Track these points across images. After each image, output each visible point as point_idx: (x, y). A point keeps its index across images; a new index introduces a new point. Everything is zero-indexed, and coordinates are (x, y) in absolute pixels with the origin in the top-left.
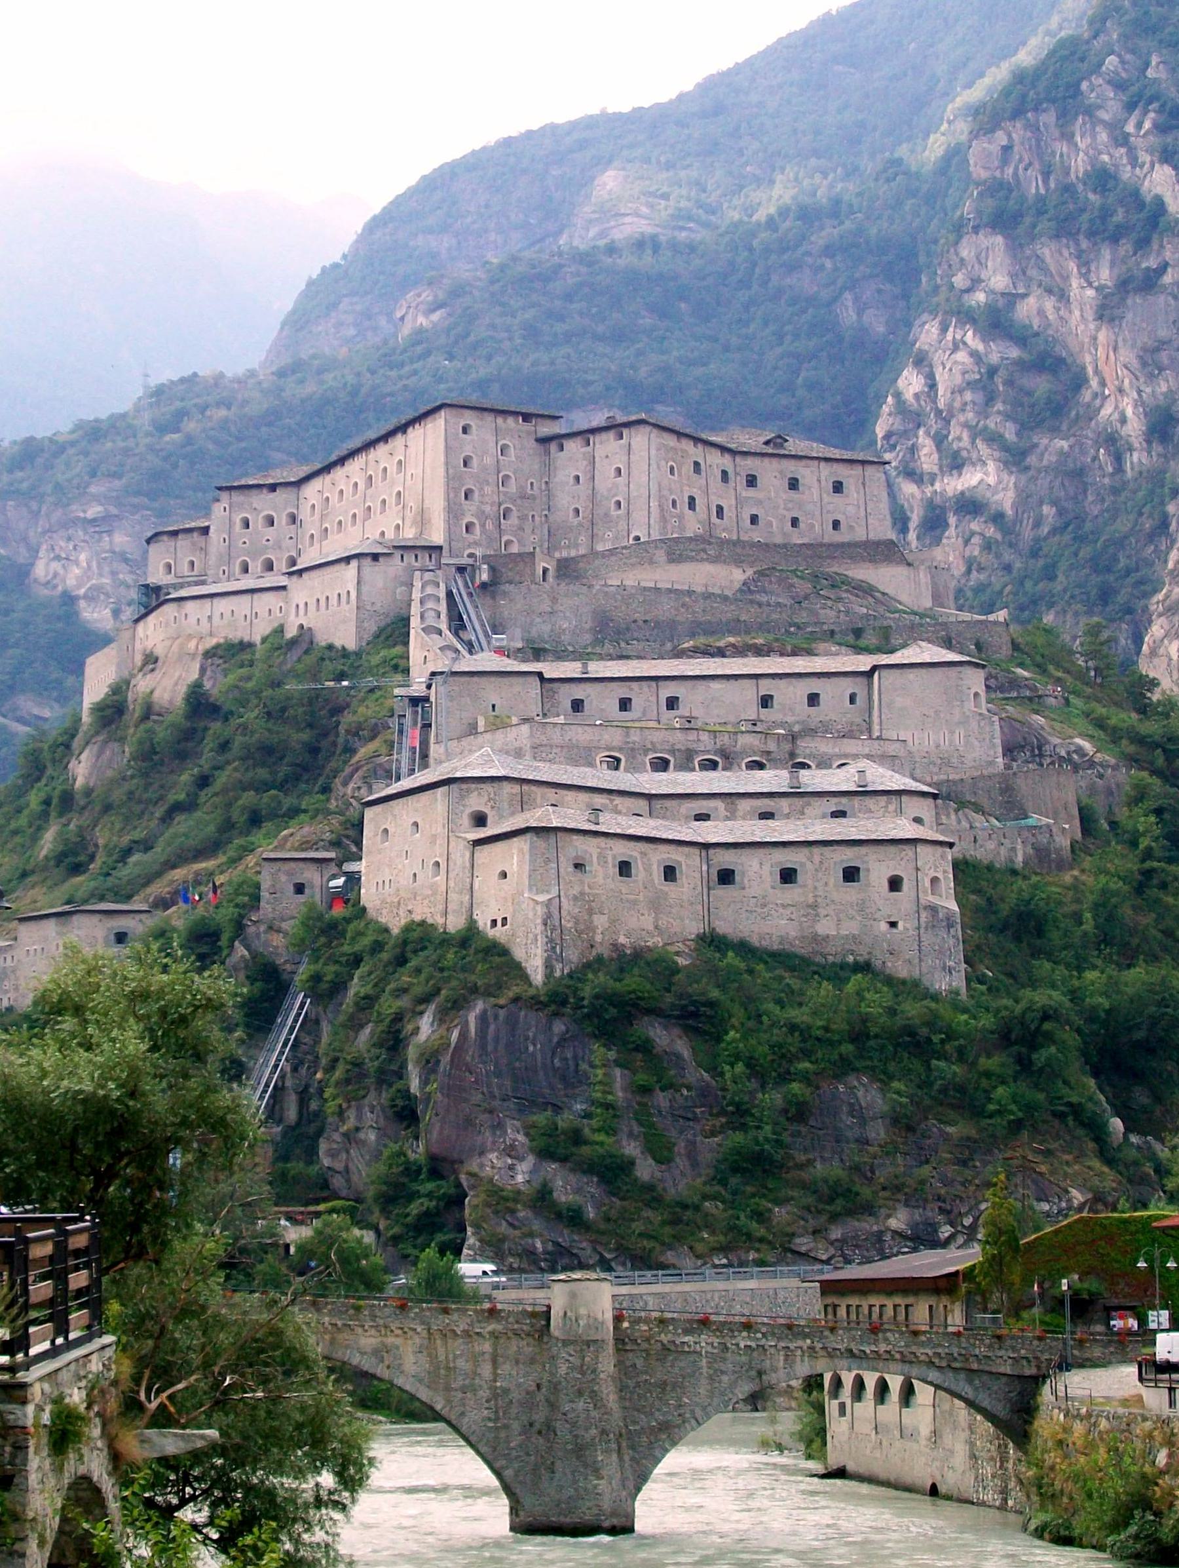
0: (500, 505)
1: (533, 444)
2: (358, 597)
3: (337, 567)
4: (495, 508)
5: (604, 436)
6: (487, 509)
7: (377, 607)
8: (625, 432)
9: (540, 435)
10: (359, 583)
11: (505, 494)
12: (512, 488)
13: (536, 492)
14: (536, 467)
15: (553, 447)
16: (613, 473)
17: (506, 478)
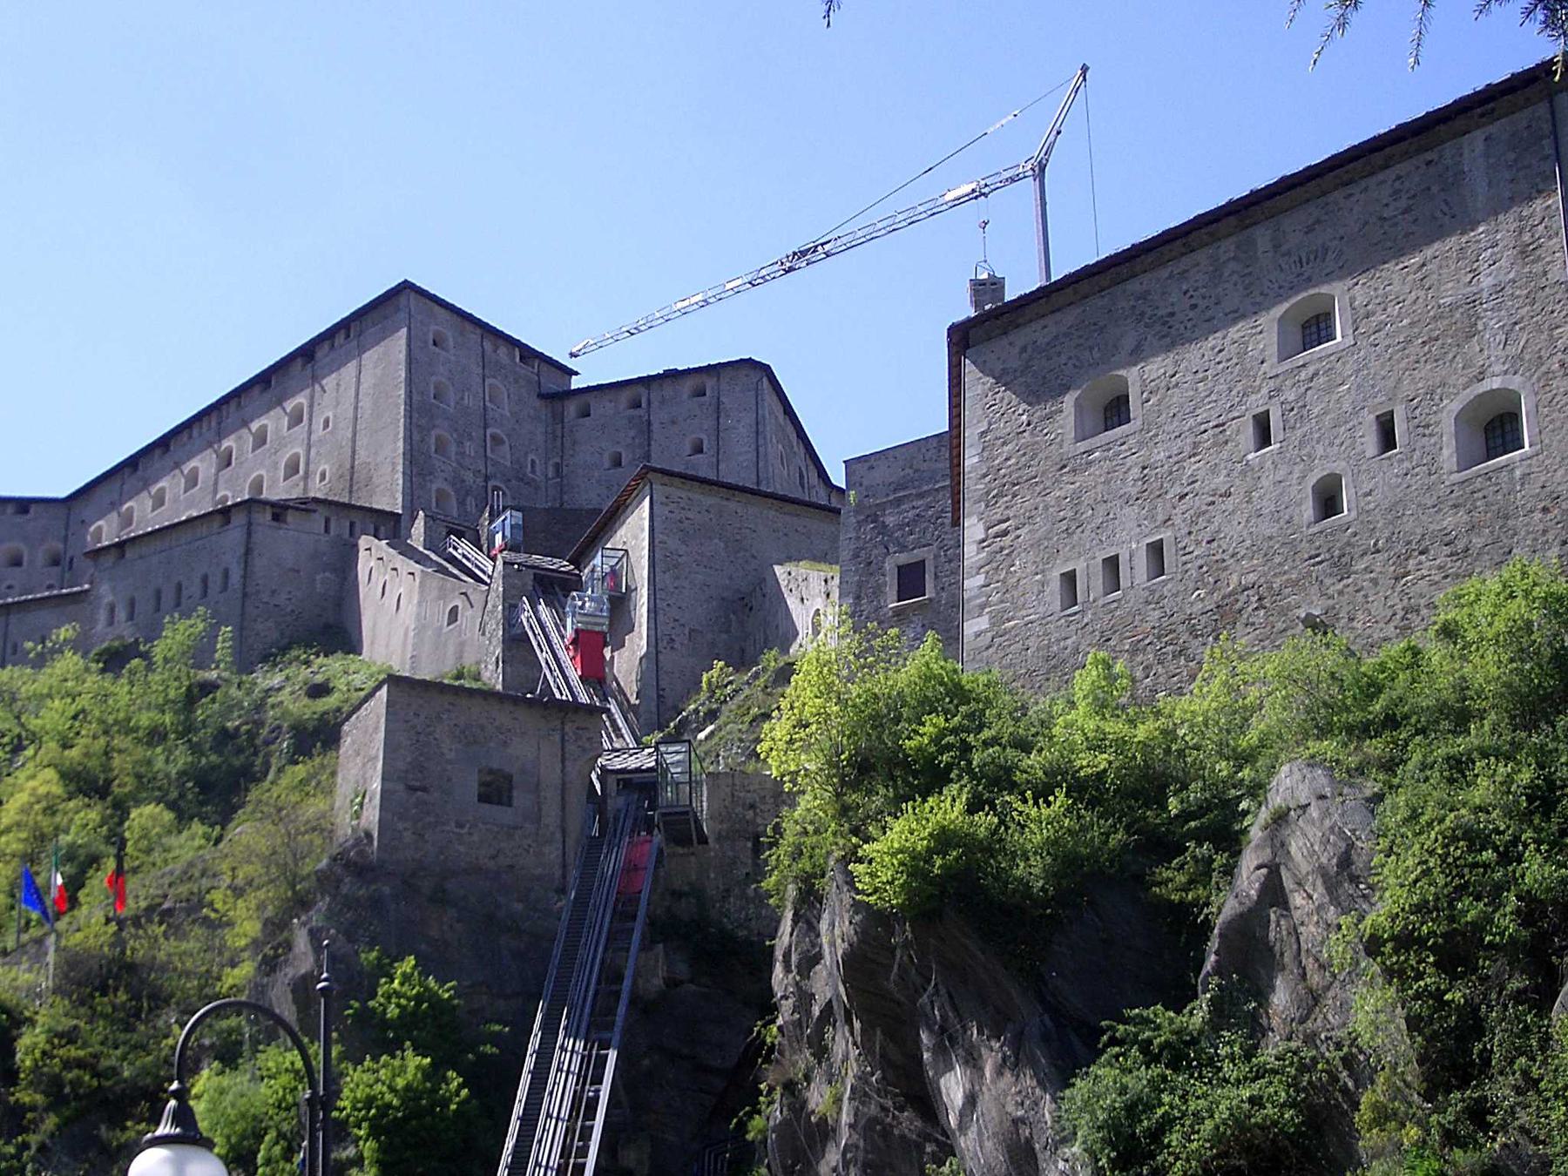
0: (487, 478)
1: (538, 403)
2: (245, 577)
3: (203, 530)
4: (480, 481)
5: (668, 389)
6: (469, 477)
7: (281, 599)
8: (710, 383)
9: (543, 391)
10: (248, 552)
11: (496, 463)
12: (504, 456)
13: (539, 477)
14: (540, 438)
15: (572, 408)
16: (688, 449)
17: (494, 437)
